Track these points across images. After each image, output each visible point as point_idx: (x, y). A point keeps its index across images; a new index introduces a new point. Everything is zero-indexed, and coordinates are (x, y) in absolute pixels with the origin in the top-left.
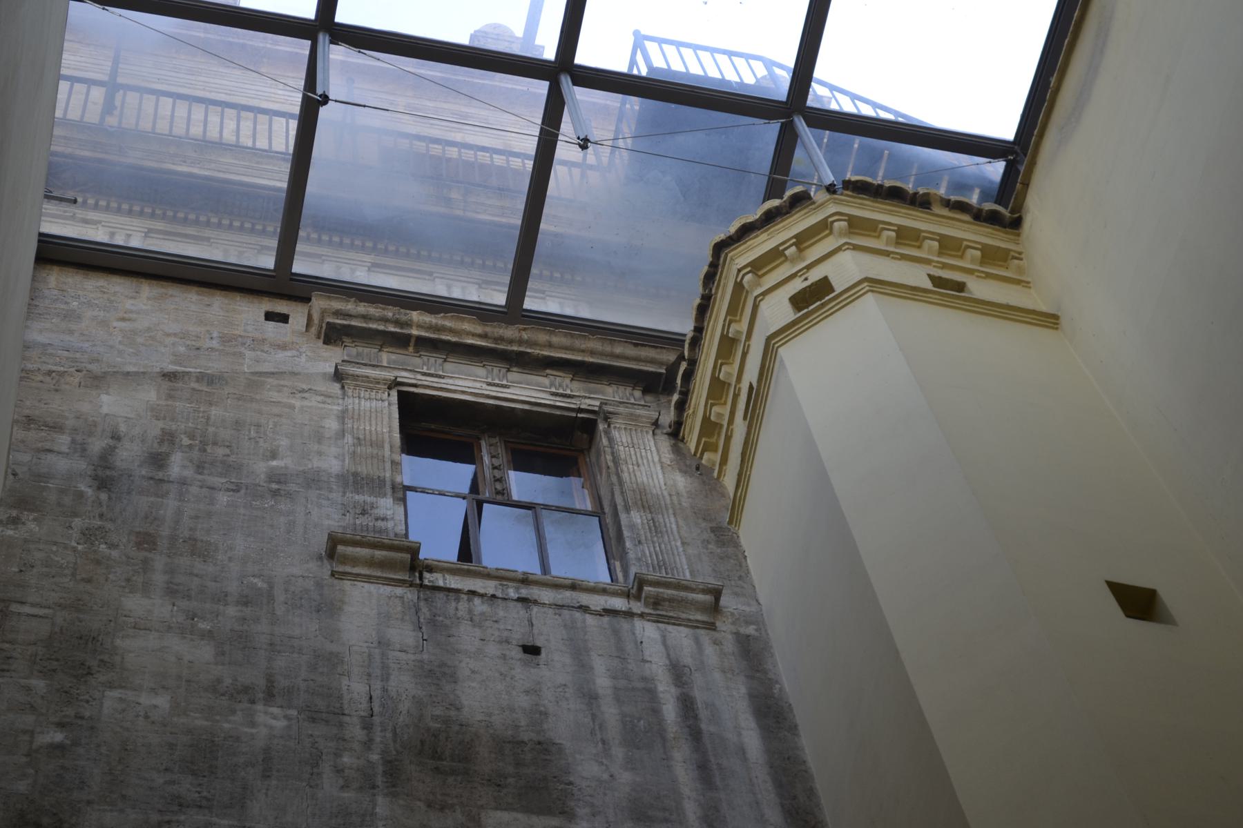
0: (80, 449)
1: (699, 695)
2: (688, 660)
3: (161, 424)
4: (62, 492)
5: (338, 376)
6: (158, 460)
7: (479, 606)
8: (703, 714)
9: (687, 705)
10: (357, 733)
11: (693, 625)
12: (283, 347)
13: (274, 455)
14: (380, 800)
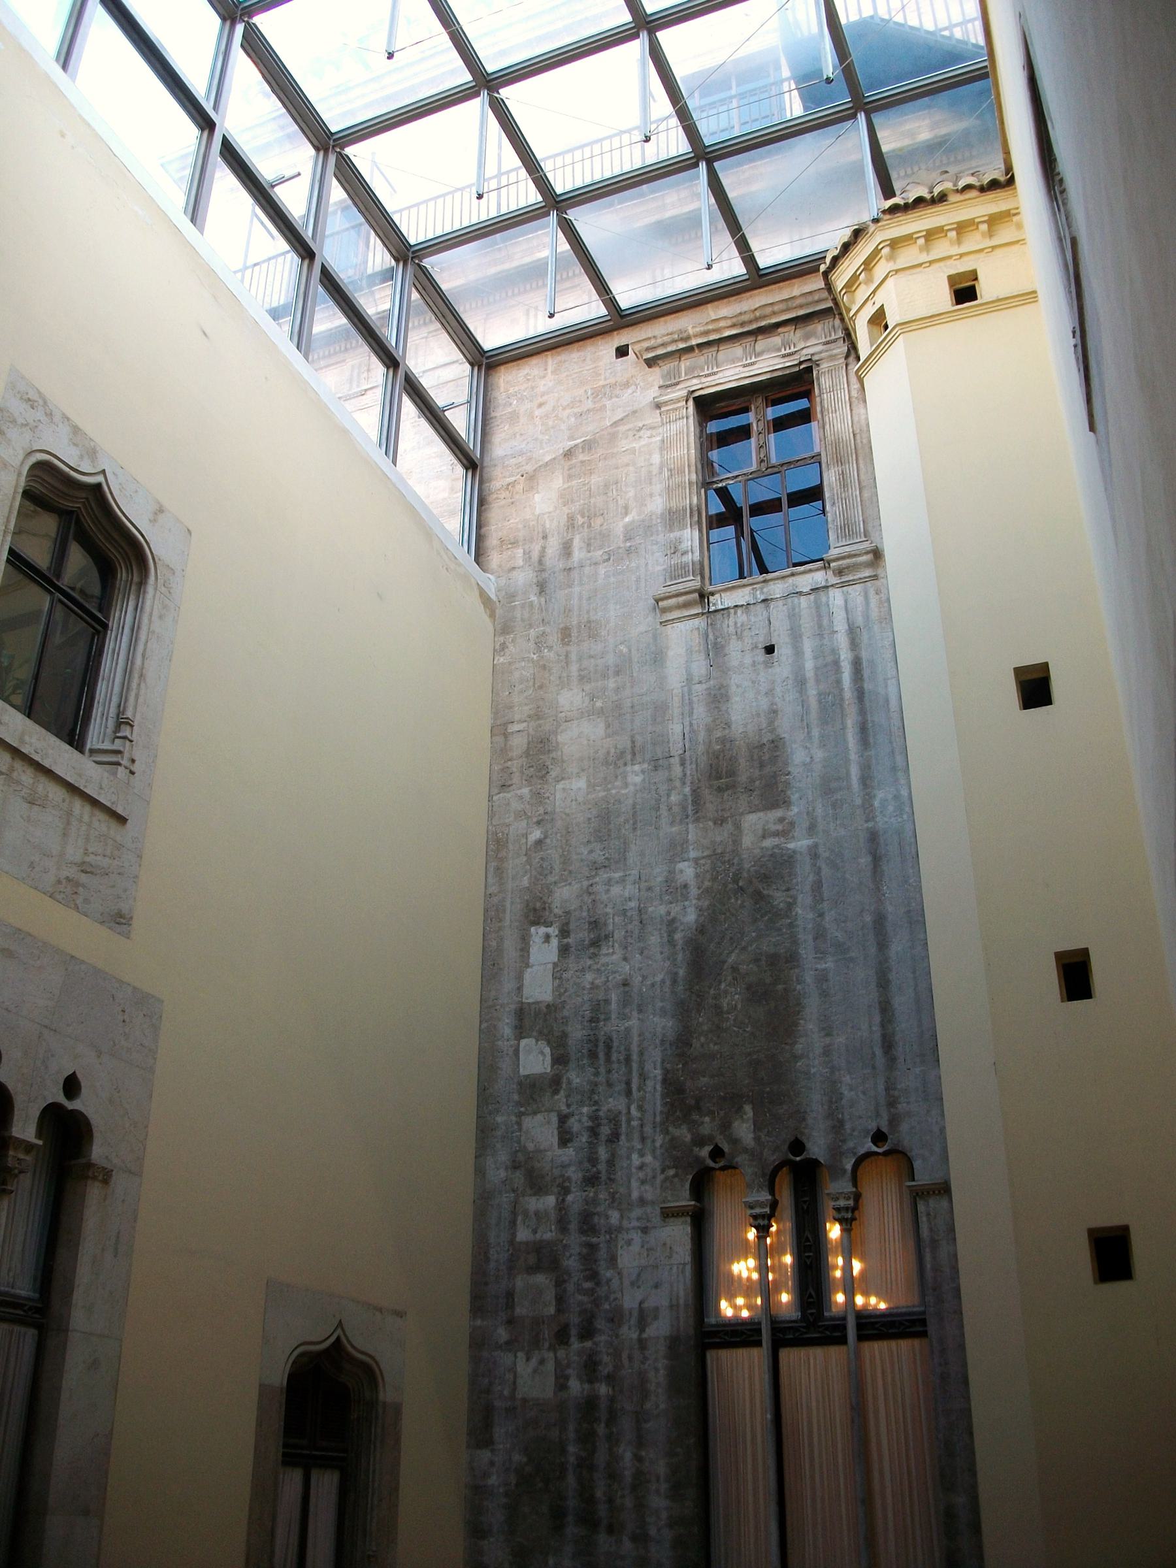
0: (527, 554)
1: (864, 655)
2: (860, 621)
3: (566, 510)
4: (523, 606)
5: (658, 406)
7: (741, 617)
8: (866, 673)
9: (857, 664)
10: (677, 770)
11: (863, 581)
12: (627, 385)
13: (626, 510)
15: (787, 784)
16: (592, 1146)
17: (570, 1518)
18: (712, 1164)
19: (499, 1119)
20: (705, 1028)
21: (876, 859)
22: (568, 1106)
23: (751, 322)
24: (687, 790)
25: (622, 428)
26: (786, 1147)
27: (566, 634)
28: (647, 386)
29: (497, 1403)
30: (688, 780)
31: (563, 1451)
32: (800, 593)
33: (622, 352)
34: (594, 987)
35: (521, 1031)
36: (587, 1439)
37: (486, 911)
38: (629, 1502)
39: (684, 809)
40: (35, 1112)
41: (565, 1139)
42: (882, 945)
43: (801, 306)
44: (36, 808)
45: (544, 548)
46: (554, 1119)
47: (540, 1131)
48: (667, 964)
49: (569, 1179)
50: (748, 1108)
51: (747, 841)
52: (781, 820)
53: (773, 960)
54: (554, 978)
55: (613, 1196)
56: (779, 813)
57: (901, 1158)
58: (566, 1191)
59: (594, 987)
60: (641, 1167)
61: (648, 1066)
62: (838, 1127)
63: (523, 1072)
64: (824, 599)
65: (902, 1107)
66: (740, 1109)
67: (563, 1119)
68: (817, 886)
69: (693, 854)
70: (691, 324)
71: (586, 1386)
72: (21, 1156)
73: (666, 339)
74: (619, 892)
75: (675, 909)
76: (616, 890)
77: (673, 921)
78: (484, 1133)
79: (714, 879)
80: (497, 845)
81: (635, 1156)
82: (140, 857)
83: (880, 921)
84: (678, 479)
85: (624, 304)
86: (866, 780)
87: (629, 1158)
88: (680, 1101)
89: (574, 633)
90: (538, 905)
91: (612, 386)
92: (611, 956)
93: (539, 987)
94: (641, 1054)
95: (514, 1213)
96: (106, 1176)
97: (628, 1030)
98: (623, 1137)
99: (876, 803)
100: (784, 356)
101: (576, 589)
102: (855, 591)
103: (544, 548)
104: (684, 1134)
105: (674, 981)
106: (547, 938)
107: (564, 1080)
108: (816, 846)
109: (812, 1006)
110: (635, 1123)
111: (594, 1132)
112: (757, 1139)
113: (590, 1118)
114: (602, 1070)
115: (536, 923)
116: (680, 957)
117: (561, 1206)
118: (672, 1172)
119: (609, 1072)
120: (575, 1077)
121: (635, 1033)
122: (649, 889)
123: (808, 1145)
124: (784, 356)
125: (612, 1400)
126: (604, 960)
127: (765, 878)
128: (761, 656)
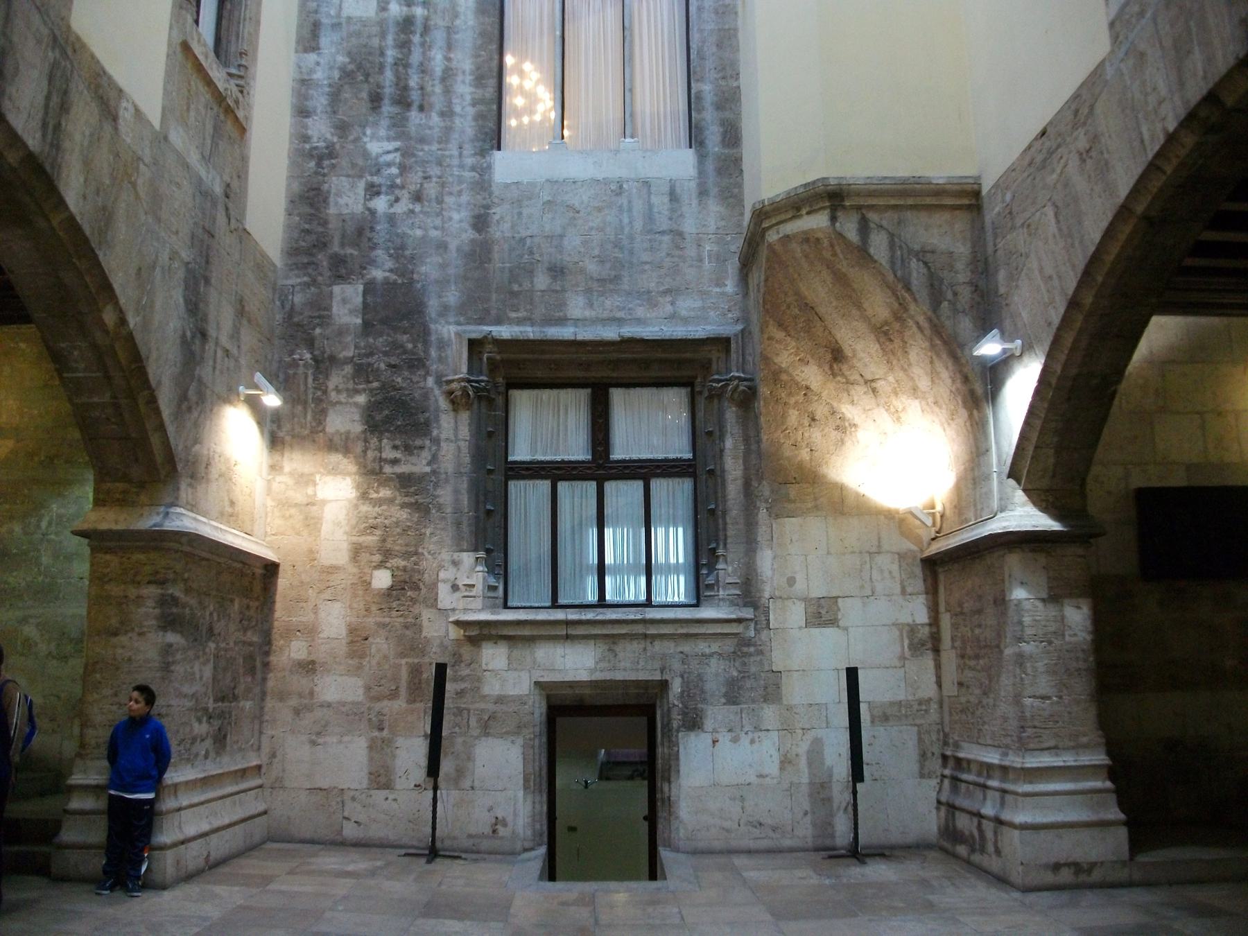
17: (386, 101)
29: (325, 21)
31: (382, 54)
36: (404, 45)
38: (438, 89)
71: (405, 9)
125: (427, 19)
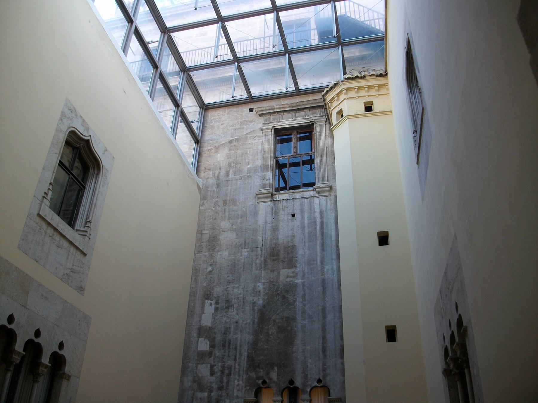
0: (214, 174)
1: (325, 220)
2: (324, 209)
4: (211, 191)
5: (262, 130)
6: (227, 174)
7: (285, 203)
8: (325, 226)
9: (322, 224)
10: (259, 252)
11: (326, 196)
12: (252, 121)
13: (248, 164)
14: (263, 272)
15: (296, 260)
16: (222, 377)
18: (262, 386)
19: (190, 365)
20: (263, 340)
21: (324, 289)
22: (214, 362)
23: (295, 106)
24: (262, 259)
25: (249, 136)
26: (288, 382)
27: (225, 202)
28: (259, 123)
30: (263, 256)
32: (305, 198)
33: (251, 110)
34: (226, 322)
35: (199, 335)
37: (190, 293)
39: (261, 265)
40: (49, 354)
41: (212, 373)
42: (324, 317)
43: (312, 104)
44: (59, 249)
45: (219, 172)
46: (209, 366)
47: (204, 370)
48: (251, 317)
49: (213, 387)
50: (276, 368)
51: (281, 278)
52: (293, 272)
53: (288, 319)
54: (212, 318)
55: (228, 394)
56: (293, 270)
57: (327, 390)
58: (212, 391)
59: (226, 322)
60: (238, 385)
61: (243, 351)
62: (306, 377)
63: (199, 349)
64: (313, 201)
65: (328, 371)
66: (273, 368)
67: (212, 367)
68: (304, 296)
69: (263, 281)
70: (275, 104)
72: (43, 369)
73: (267, 108)
74: (236, 291)
75: (255, 299)
76: (236, 290)
77: (255, 303)
78: (184, 369)
79: (269, 290)
80: (196, 271)
81: (236, 381)
82: (89, 268)
83: (324, 309)
84: (267, 155)
85: (253, 95)
86: (322, 262)
87: (234, 382)
88: (253, 364)
89: (228, 203)
90: (208, 293)
91: (247, 121)
92: (232, 312)
93: (207, 321)
94: (241, 346)
95: (193, 398)
96: (69, 378)
97: (237, 338)
98: (232, 375)
99: (325, 270)
100: (305, 119)
101: (230, 188)
102: (323, 199)
103: (219, 172)
104: (253, 375)
105: (254, 323)
106: (211, 304)
107: (213, 353)
108: (304, 282)
109: (300, 335)
110: (237, 370)
111: (222, 372)
112: (278, 379)
113: (221, 367)
114: (227, 351)
115: (207, 299)
116: (256, 315)
117: (209, 396)
118: (248, 388)
119: (229, 352)
120: (217, 353)
121: (239, 339)
122: (247, 291)
123: (295, 382)
124: (305, 119)
126: (230, 314)
127: (287, 291)
128: (290, 217)
